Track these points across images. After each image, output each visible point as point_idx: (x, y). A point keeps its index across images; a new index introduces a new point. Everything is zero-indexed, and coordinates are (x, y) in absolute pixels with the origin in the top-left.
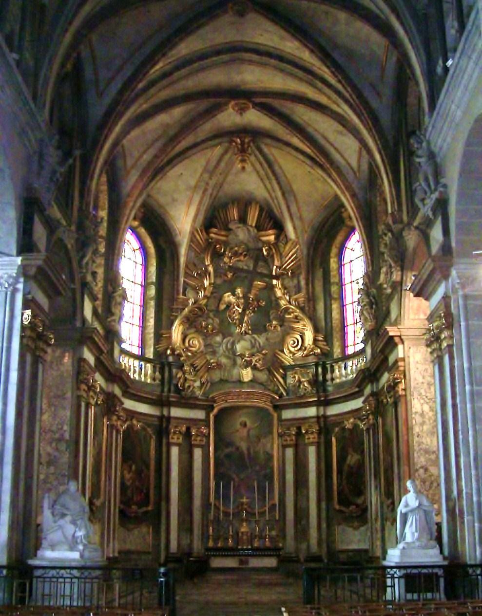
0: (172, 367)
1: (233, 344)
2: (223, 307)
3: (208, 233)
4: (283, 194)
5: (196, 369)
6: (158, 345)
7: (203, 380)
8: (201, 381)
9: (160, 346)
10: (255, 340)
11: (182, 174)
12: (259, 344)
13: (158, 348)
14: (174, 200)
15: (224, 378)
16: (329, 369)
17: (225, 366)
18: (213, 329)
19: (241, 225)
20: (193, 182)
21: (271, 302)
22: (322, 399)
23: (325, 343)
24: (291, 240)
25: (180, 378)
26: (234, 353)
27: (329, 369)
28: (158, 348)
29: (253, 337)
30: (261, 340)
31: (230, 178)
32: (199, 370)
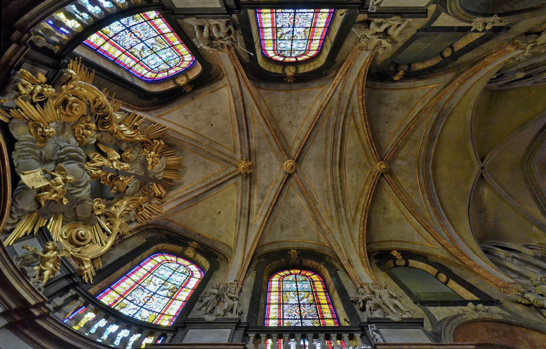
0: (52, 70)
1: (77, 159)
2: (102, 148)
3: (158, 139)
4: (196, 197)
5: (38, 106)
6: (82, 63)
7: (13, 112)
8: (13, 108)
9: (80, 63)
10: (84, 187)
11: (212, 125)
12: (78, 193)
13: (78, 60)
14: (186, 117)
15: (17, 147)
16: (69, 295)
17: (41, 148)
18: (86, 136)
19: (164, 166)
20: (202, 132)
21: (113, 198)
22: (37, 313)
23: (94, 274)
24: (161, 207)
25: (37, 77)
26: (62, 160)
27: (69, 295)
28: (78, 60)
29: (86, 185)
30: (85, 193)
31: (201, 159)
32: (36, 108)
